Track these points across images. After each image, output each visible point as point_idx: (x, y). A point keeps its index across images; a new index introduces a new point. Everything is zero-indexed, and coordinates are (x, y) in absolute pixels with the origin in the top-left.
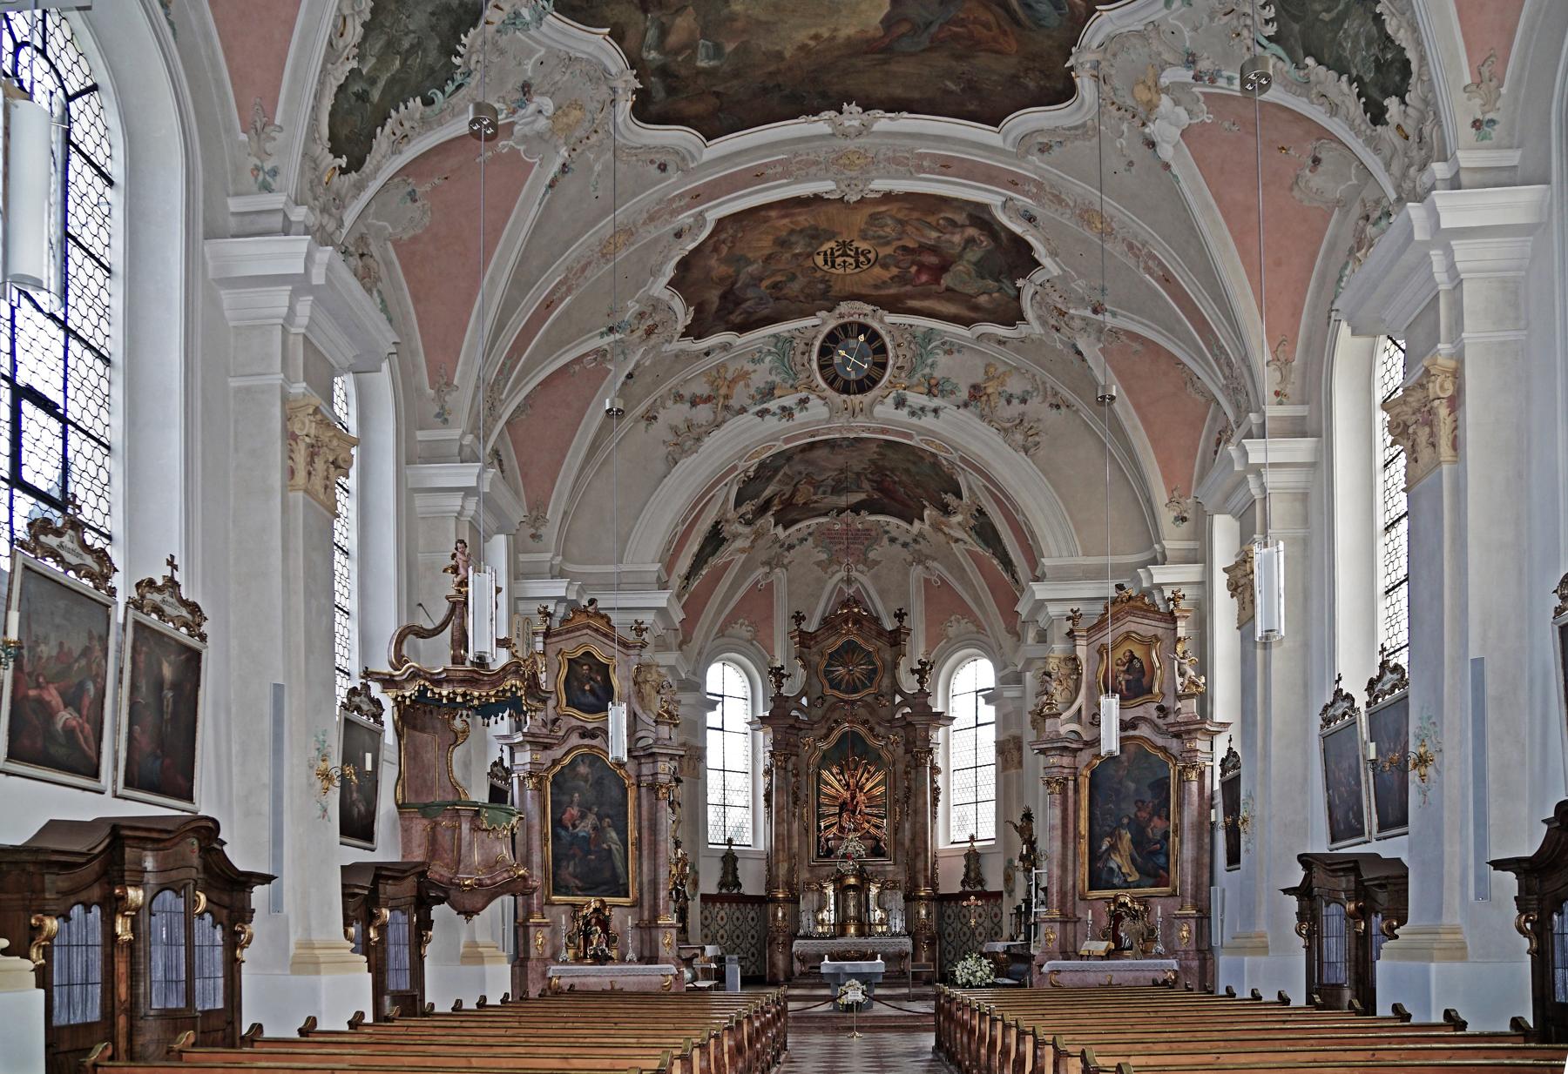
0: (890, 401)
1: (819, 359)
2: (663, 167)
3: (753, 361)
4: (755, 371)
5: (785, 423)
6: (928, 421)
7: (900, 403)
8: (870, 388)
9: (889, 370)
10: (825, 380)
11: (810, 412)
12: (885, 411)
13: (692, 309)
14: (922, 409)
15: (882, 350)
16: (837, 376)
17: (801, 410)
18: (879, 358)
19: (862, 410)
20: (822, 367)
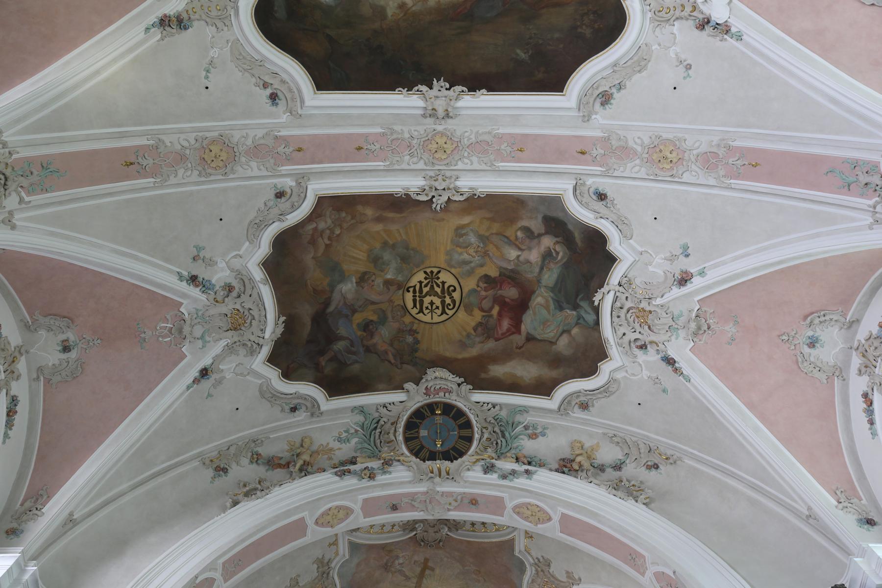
0: (478, 468)
1: (405, 432)
2: (274, 97)
3: (340, 440)
4: (340, 449)
5: (366, 483)
6: (521, 482)
7: (489, 469)
8: (456, 459)
9: (475, 443)
10: (411, 451)
11: (393, 475)
12: (476, 474)
13: (283, 319)
14: (514, 473)
15: (468, 425)
16: (422, 447)
17: (385, 473)
18: (465, 433)
19: (448, 474)
20: (407, 440)
